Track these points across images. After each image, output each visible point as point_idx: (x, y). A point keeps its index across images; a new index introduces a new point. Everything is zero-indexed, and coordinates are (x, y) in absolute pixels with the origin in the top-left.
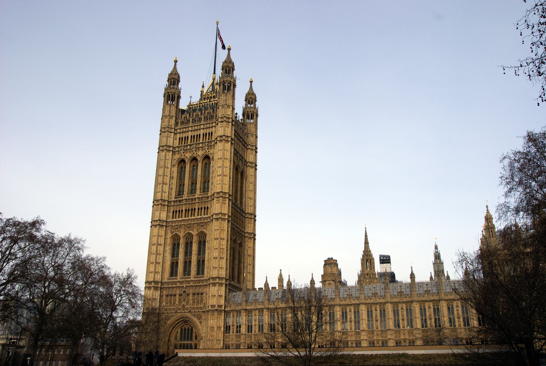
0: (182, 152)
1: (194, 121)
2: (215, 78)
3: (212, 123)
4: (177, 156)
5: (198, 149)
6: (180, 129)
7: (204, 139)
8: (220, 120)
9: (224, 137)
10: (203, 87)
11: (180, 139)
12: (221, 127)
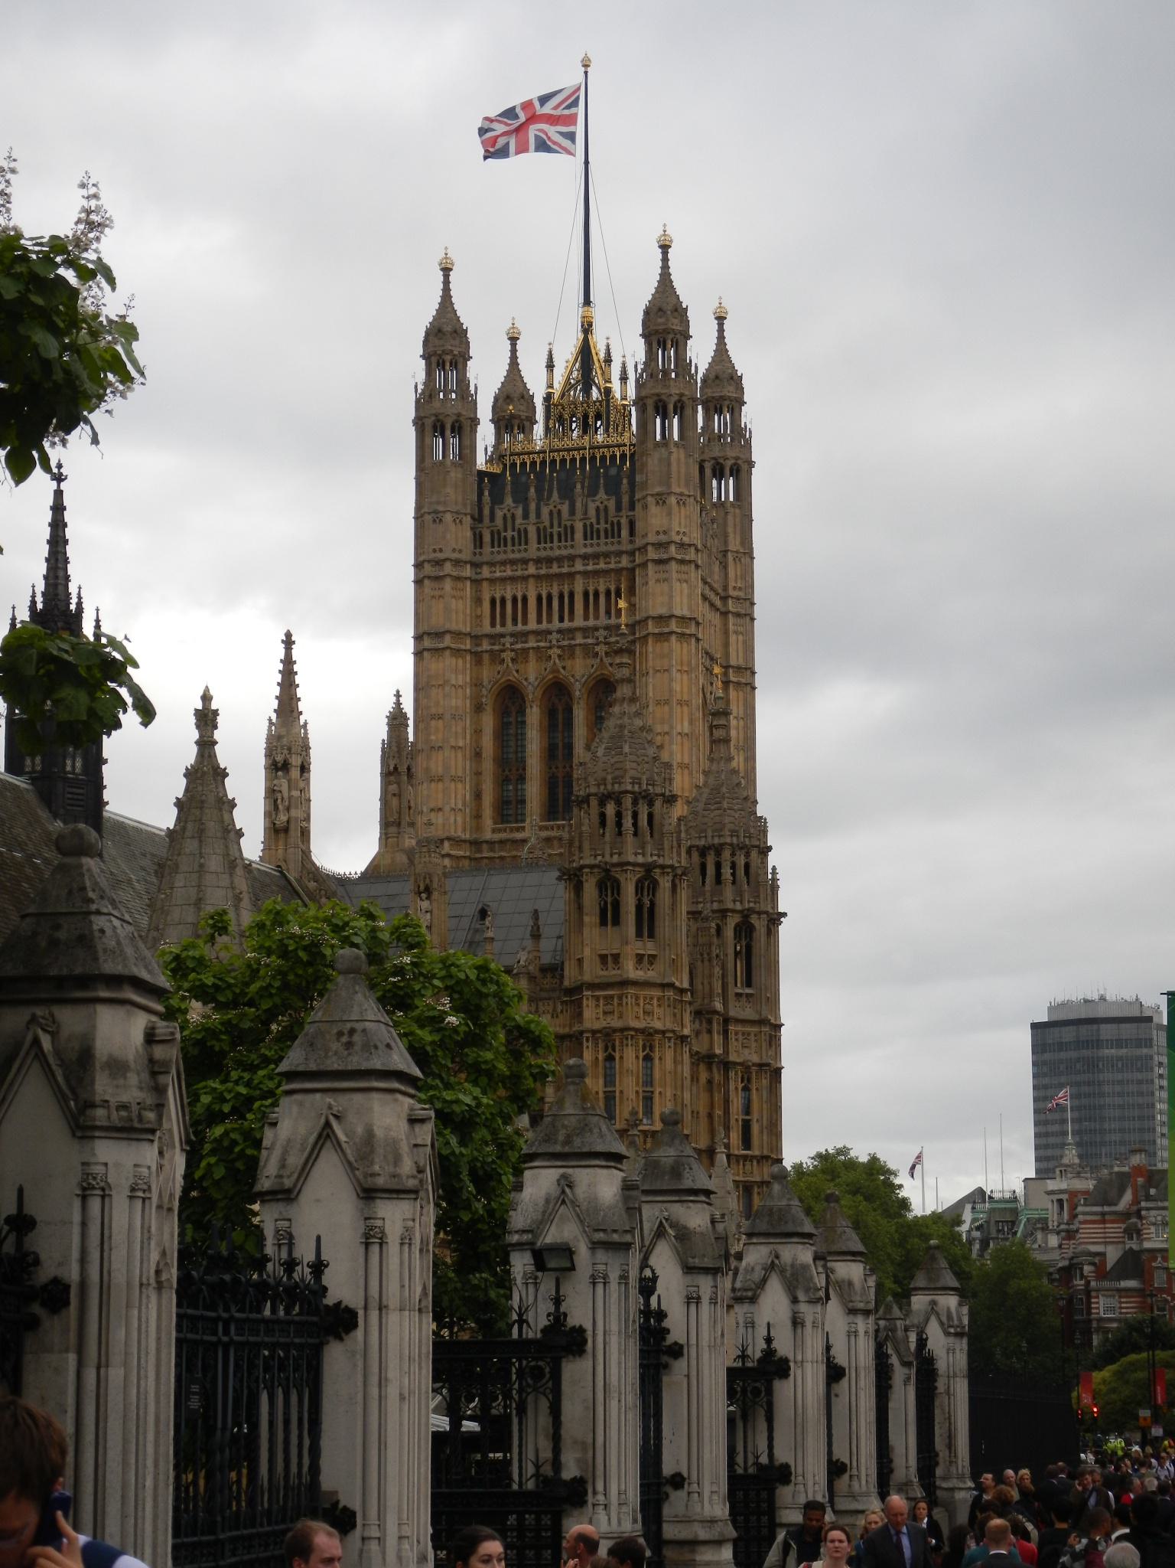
0: (507, 656)
1: (544, 536)
2: (590, 325)
3: (619, 554)
4: (487, 673)
5: (569, 652)
6: (492, 564)
7: (591, 616)
8: (652, 554)
9: (673, 626)
10: (550, 366)
11: (493, 601)
12: (658, 581)
